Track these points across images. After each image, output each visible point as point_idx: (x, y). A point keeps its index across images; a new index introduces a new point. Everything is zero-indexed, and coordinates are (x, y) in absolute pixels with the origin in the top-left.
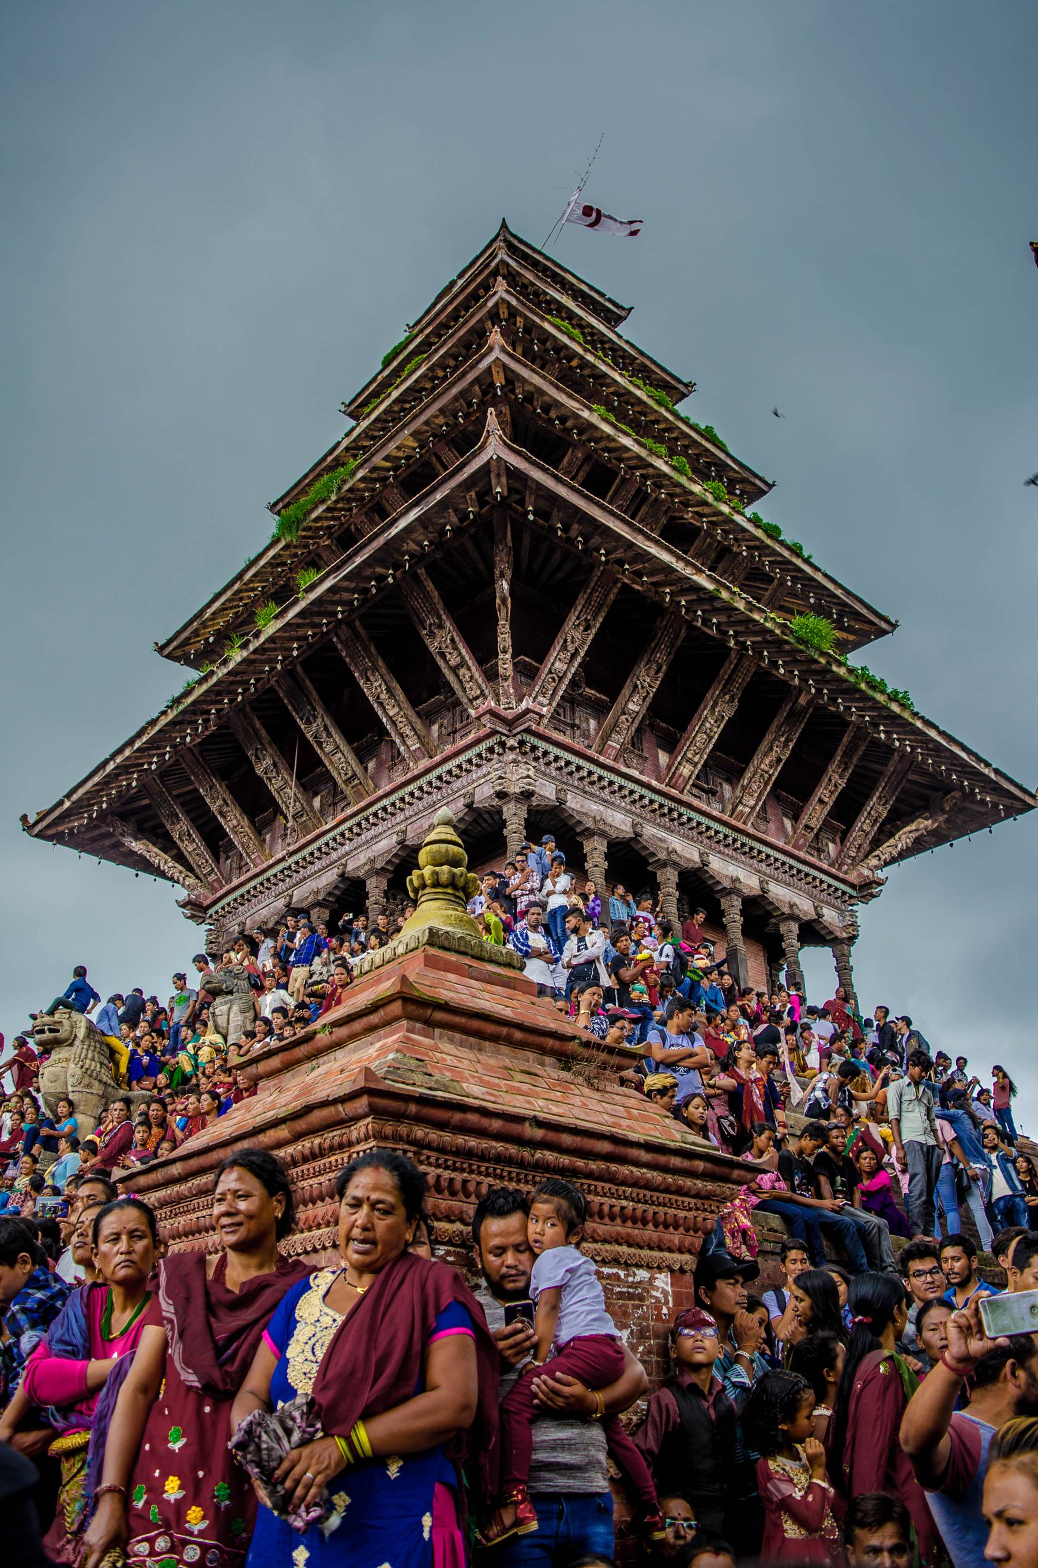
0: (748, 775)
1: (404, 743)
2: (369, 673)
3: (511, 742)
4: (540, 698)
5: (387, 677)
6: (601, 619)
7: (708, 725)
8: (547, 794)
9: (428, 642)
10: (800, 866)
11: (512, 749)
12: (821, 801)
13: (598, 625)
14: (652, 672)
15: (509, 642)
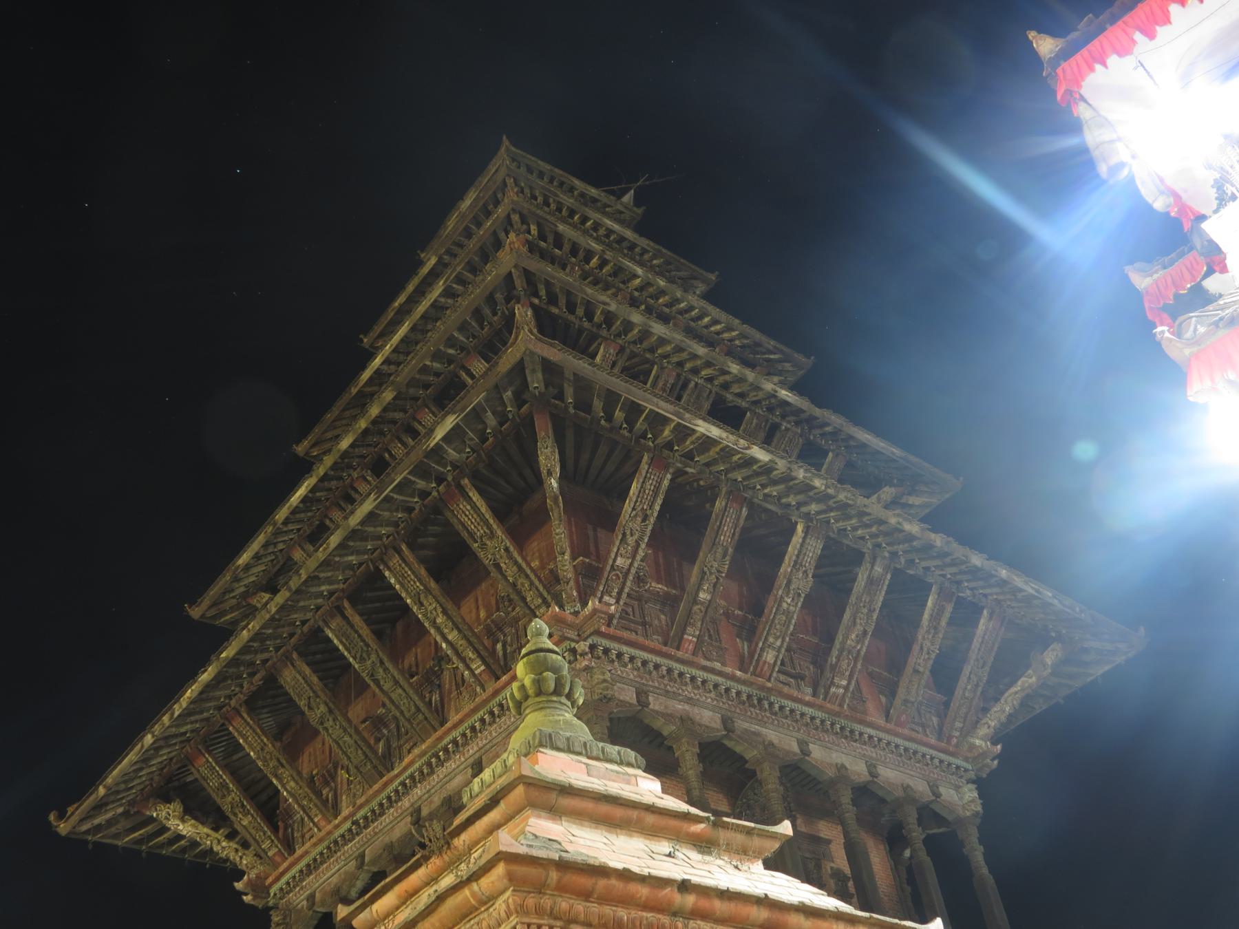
0: (835, 653)
1: (468, 667)
2: (422, 597)
3: (583, 646)
4: (606, 598)
5: (442, 600)
6: (657, 508)
7: (785, 605)
8: (628, 699)
9: (481, 555)
10: (907, 744)
11: (583, 654)
12: (916, 671)
13: (656, 514)
14: (719, 556)
15: (566, 544)
